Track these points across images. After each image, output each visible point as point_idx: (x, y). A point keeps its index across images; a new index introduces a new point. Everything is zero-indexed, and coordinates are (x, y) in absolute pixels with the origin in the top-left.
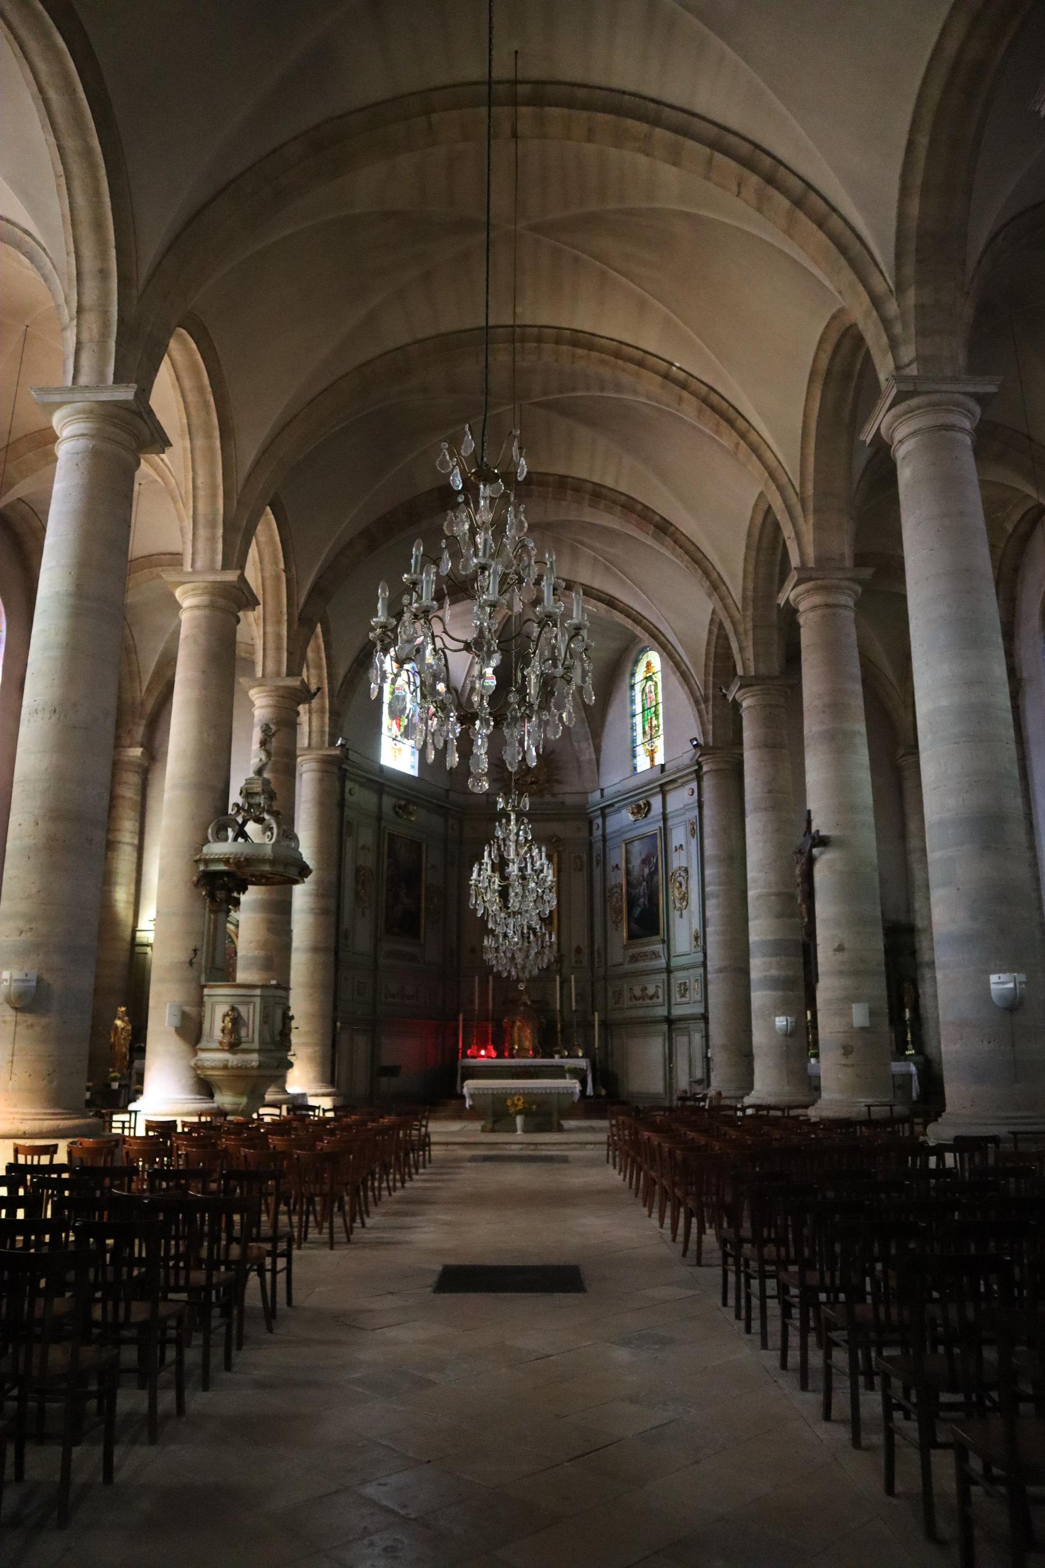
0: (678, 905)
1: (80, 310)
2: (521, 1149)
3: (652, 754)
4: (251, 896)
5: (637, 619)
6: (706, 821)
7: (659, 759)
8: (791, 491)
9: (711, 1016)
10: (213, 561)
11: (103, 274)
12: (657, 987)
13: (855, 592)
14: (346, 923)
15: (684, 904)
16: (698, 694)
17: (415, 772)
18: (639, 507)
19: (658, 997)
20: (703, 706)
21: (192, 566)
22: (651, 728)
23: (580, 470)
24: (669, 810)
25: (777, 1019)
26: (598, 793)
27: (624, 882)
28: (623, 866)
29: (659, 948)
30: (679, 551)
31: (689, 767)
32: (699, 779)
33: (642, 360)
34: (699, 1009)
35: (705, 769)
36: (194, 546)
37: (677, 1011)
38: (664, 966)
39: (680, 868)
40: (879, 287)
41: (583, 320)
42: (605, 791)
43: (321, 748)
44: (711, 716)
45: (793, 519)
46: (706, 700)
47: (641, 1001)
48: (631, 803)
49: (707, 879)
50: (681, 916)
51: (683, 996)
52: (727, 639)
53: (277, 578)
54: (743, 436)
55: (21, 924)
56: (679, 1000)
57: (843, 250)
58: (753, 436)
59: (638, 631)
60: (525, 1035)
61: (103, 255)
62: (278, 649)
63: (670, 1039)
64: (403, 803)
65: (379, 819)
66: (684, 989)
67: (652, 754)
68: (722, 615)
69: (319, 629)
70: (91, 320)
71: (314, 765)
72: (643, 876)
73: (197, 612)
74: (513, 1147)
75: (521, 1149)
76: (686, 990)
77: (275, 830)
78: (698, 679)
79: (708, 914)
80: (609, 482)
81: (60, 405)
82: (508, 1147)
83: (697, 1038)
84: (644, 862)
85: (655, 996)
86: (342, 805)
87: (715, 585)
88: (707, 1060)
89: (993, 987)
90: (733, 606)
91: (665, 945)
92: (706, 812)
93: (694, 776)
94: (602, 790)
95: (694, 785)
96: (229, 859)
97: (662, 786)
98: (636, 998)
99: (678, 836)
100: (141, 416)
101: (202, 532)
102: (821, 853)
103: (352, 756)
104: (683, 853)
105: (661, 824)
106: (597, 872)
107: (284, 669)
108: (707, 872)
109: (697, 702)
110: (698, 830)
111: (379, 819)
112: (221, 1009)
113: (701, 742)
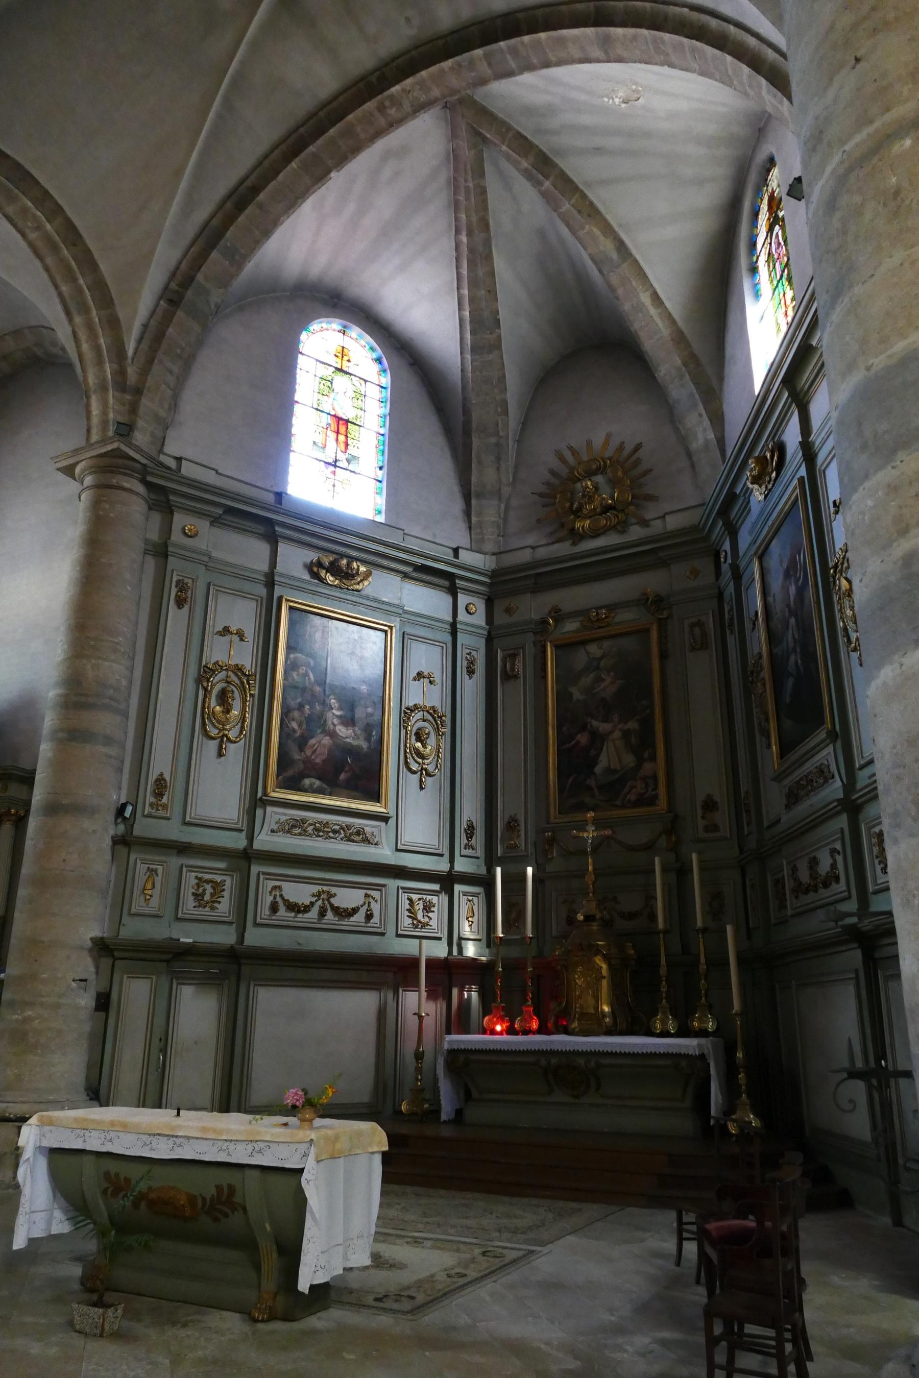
12: (833, 852)
29: (828, 755)
47: (811, 896)
72: (788, 606)
91: (839, 744)
98: (807, 891)
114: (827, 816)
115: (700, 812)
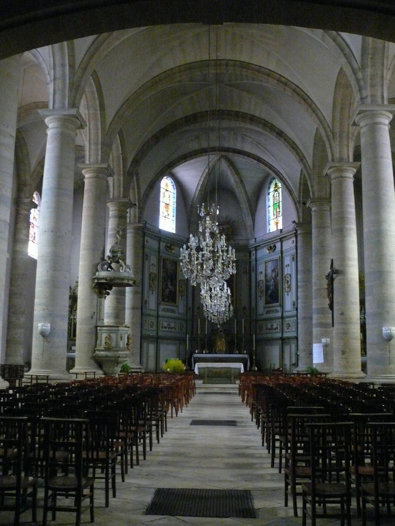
0: (287, 290)
1: (55, 79)
2: (218, 390)
3: (277, 223)
4: (112, 292)
5: (270, 167)
6: (299, 255)
7: (280, 227)
8: (328, 130)
9: (299, 337)
10: (97, 159)
11: (63, 65)
13: (353, 171)
14: (146, 298)
15: (289, 290)
16: (296, 200)
17: (174, 231)
18: (270, 125)
19: (278, 329)
20: (298, 205)
21: (89, 161)
22: (277, 212)
23: (245, 109)
24: (283, 249)
25: (322, 339)
26: (254, 240)
27: (264, 280)
28: (264, 272)
29: (279, 309)
30: (286, 143)
31: (292, 231)
32: (296, 237)
33: (269, 74)
34: (294, 334)
35: (299, 232)
36: (89, 152)
37: (286, 335)
38: (280, 316)
39: (288, 274)
40: (356, 66)
41: (245, 58)
42: (257, 239)
43: (134, 223)
44: (301, 210)
45: (329, 140)
46: (299, 202)
47: (271, 331)
48: (267, 245)
49: (299, 280)
50: (288, 295)
51: (288, 329)
52: (306, 180)
53: (118, 157)
54: (310, 106)
55: (44, 307)
56: (286, 330)
57: (342, 50)
58: (313, 106)
59: (271, 172)
60: (221, 344)
61: (63, 59)
62: (119, 186)
63: (282, 345)
64: (169, 245)
65: (159, 252)
66: (289, 325)
67: (277, 223)
68: (305, 172)
69: (135, 178)
70: (59, 82)
71: (132, 230)
73: (92, 180)
74: (216, 389)
75: (218, 390)
76: (289, 326)
77: (124, 266)
78: (296, 194)
79: (299, 294)
80: (257, 114)
81: (48, 116)
82: (214, 389)
83: (293, 346)
84: (273, 271)
85: (277, 328)
86: (143, 247)
87: (302, 159)
88: (298, 355)
89: (383, 332)
90: (309, 168)
92: (299, 251)
93: (294, 235)
94: (255, 239)
95: (294, 239)
96: (107, 278)
97: (280, 239)
98: (269, 329)
99: (287, 260)
100: (78, 118)
101: (93, 147)
102: (336, 277)
103: (148, 226)
104: (289, 268)
105: (280, 255)
106: (253, 274)
107: (122, 196)
108: (299, 276)
109: (295, 204)
110: (295, 258)
111: (159, 252)
112: (104, 335)
113: (297, 221)
114: (278, 318)
115: (242, 309)
